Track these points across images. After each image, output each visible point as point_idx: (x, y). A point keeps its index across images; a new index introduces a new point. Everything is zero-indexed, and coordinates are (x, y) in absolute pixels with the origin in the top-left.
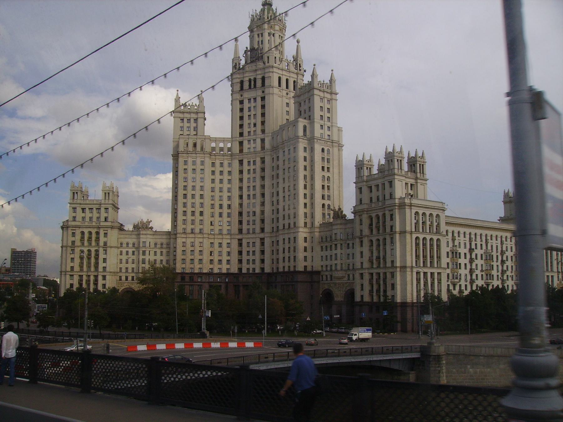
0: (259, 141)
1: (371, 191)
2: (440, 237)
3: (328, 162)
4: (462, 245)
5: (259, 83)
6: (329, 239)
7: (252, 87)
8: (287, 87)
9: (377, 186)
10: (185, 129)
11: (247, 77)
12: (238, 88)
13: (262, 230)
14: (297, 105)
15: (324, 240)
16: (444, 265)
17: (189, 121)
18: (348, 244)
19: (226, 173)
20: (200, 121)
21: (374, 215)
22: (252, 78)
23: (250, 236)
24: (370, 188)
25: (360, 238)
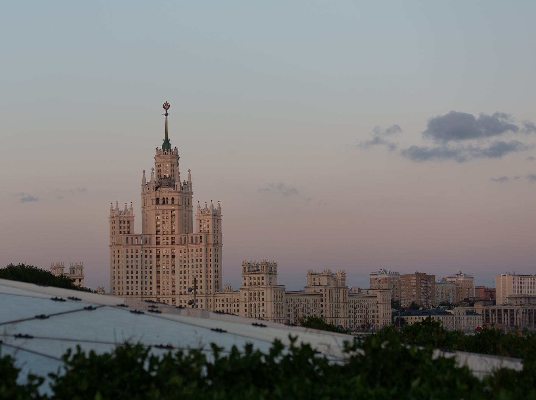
0: (170, 238)
1: (251, 280)
2: (282, 303)
3: (217, 257)
4: (291, 306)
5: (170, 202)
6: (221, 301)
7: (165, 204)
8: (185, 204)
9: (255, 279)
10: (123, 227)
11: (162, 196)
12: (155, 202)
13: (173, 293)
14: (199, 221)
15: (218, 301)
16: (284, 316)
17: (124, 222)
18: (235, 305)
19: (148, 257)
20: (130, 222)
21: (252, 292)
22: (165, 198)
23: (164, 296)
24: (251, 278)
25: (244, 302)
